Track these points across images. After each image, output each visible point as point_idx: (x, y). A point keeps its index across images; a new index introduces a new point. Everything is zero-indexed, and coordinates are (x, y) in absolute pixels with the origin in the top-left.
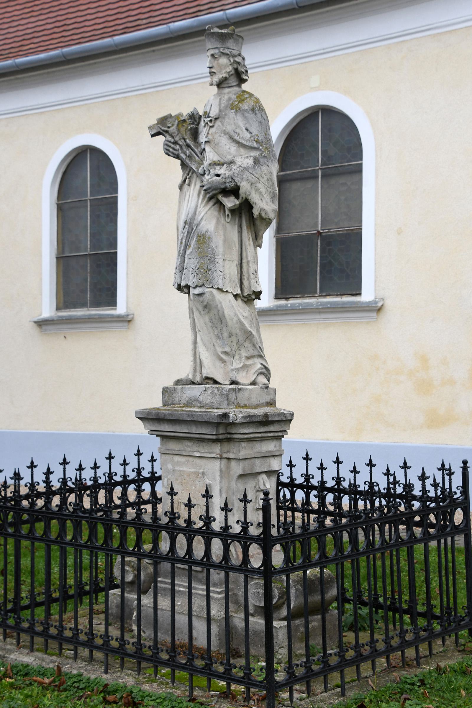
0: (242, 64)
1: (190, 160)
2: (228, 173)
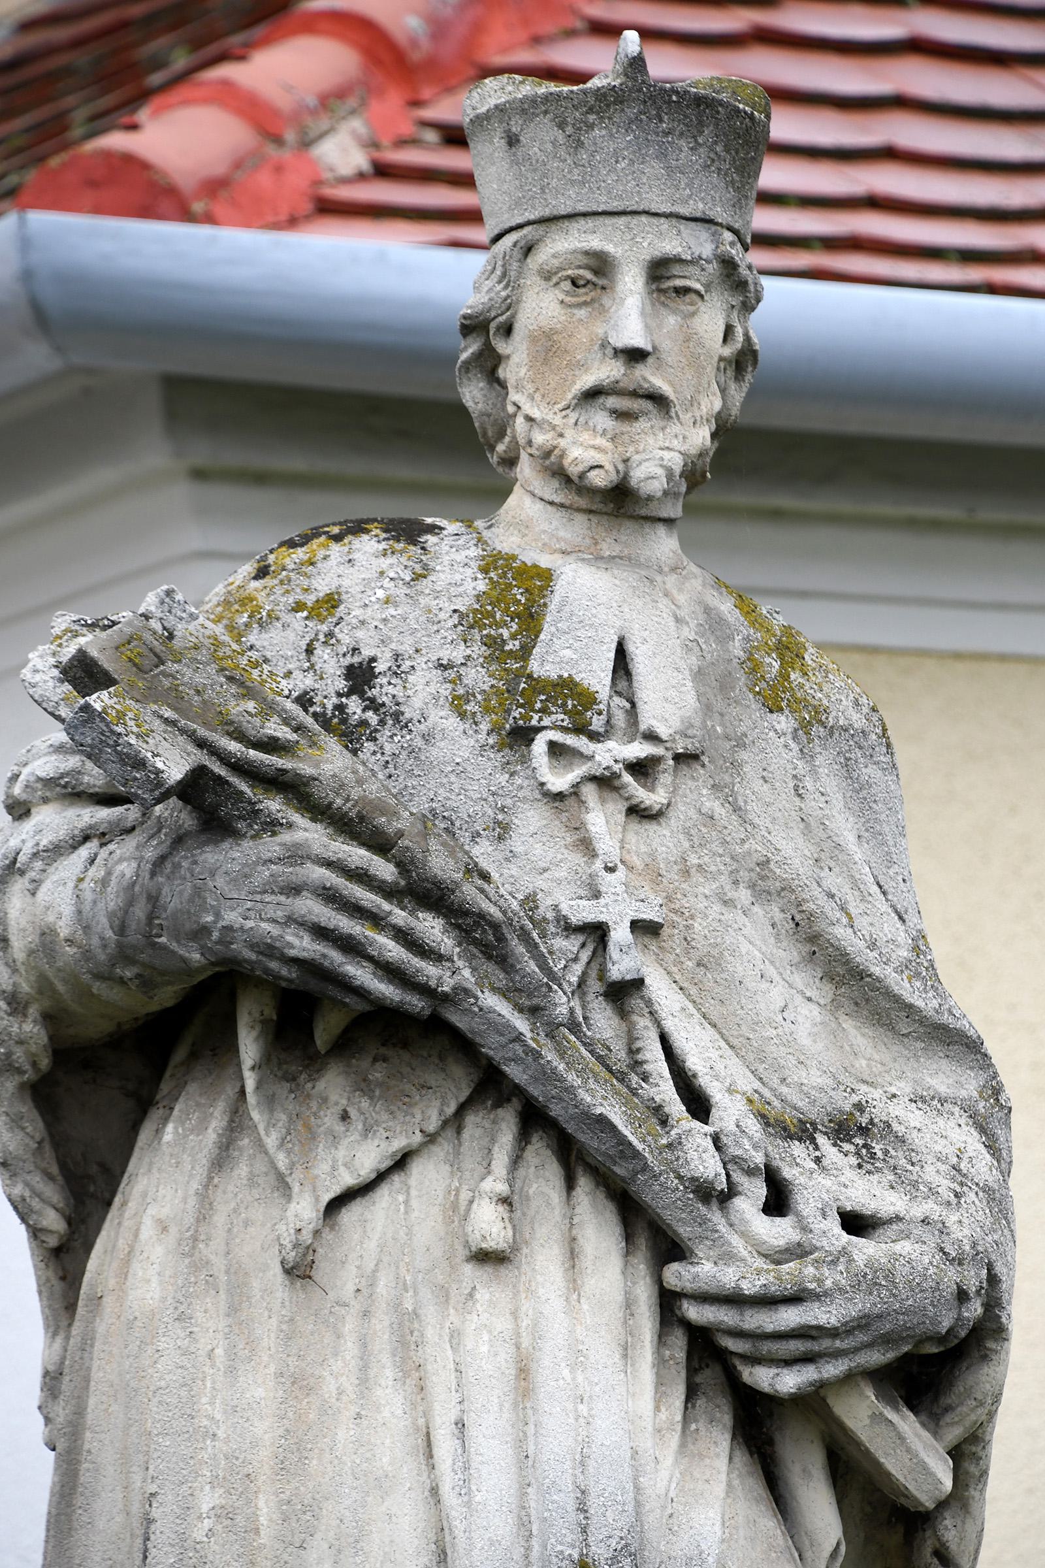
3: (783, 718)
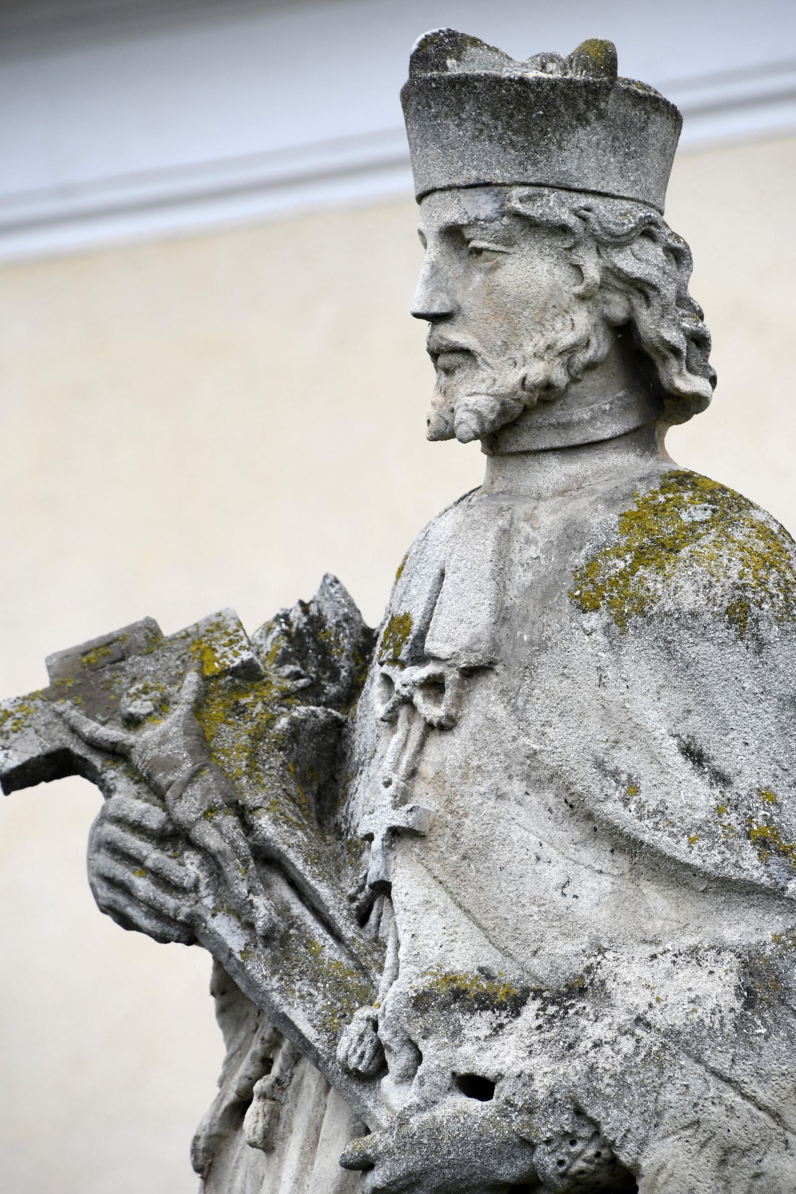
0: (669, 291)
1: (275, 965)
2: (547, 1074)
3: (595, 616)
